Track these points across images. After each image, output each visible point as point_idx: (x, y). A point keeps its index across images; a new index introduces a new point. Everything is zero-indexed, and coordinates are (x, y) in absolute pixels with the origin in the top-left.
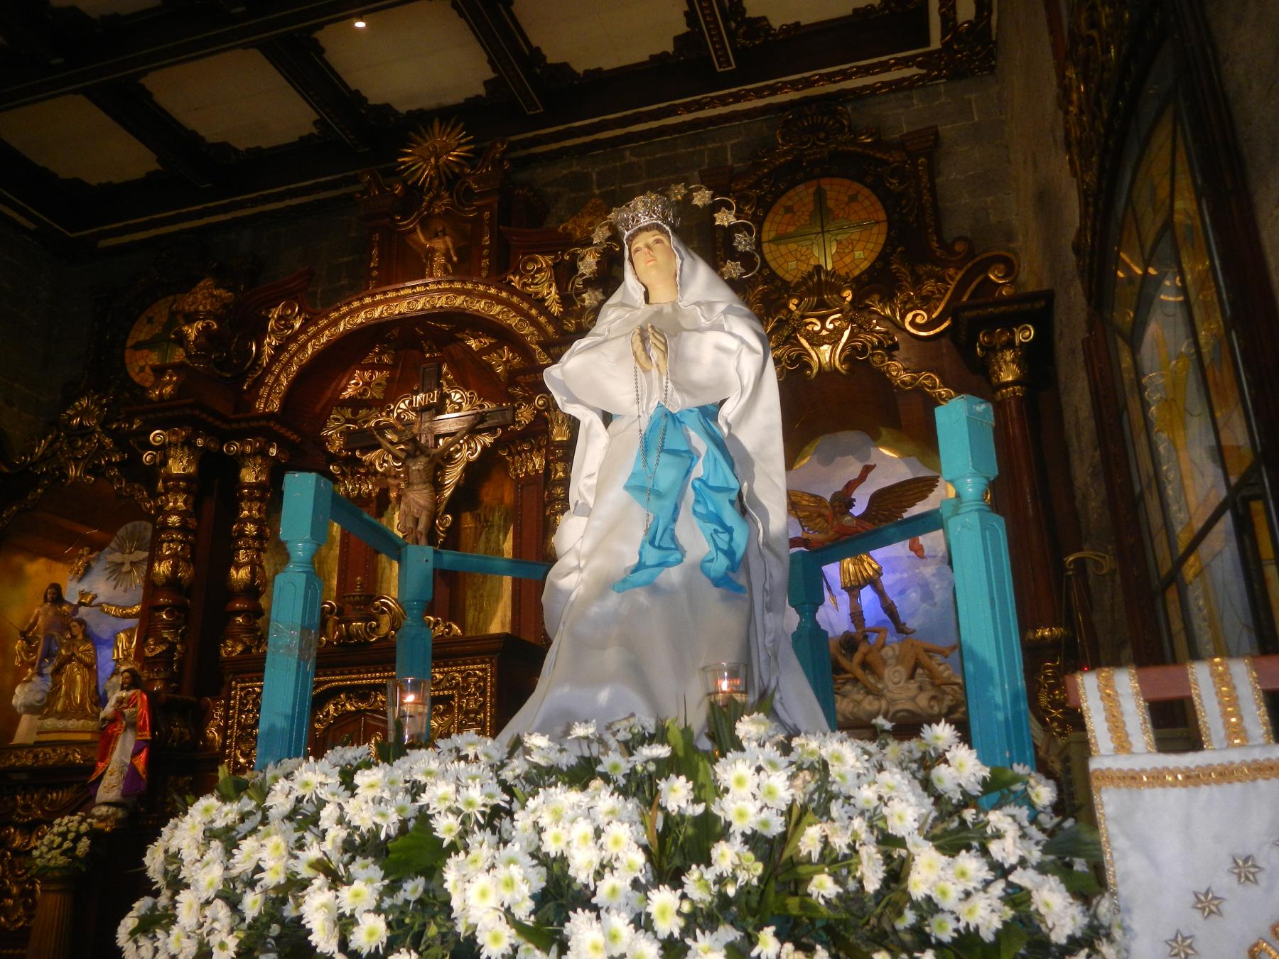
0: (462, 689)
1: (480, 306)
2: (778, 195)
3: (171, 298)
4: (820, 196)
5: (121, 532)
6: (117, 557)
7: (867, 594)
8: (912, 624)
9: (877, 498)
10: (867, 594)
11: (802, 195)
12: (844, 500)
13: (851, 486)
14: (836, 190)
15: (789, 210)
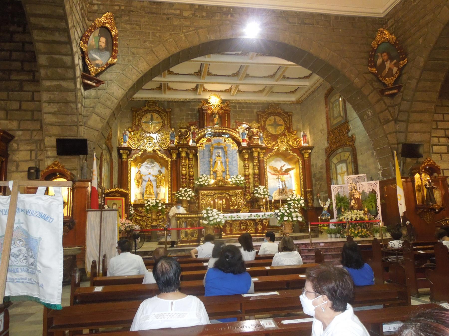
0: (238, 194)
1: (231, 133)
2: (269, 117)
3: (151, 113)
4: (275, 119)
5: (147, 160)
6: (148, 165)
7: (283, 182)
8: (287, 186)
9: (286, 170)
10: (283, 182)
11: (272, 118)
12: (281, 169)
13: (282, 167)
14: (278, 118)
15: (270, 120)
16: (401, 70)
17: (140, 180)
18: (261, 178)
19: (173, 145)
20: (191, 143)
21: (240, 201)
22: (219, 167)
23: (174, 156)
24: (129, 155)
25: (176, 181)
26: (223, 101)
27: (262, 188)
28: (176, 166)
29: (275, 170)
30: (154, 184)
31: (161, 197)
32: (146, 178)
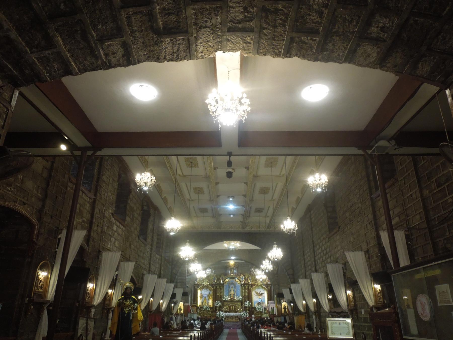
16: (278, 269)
17: (202, 296)
18: (249, 298)
19: (214, 283)
20: (221, 282)
21: (240, 307)
22: (232, 292)
23: (215, 288)
24: (198, 287)
25: (216, 298)
26: (235, 263)
27: (248, 302)
28: (215, 292)
29: (257, 293)
30: (207, 298)
31: (210, 304)
32: (204, 296)
